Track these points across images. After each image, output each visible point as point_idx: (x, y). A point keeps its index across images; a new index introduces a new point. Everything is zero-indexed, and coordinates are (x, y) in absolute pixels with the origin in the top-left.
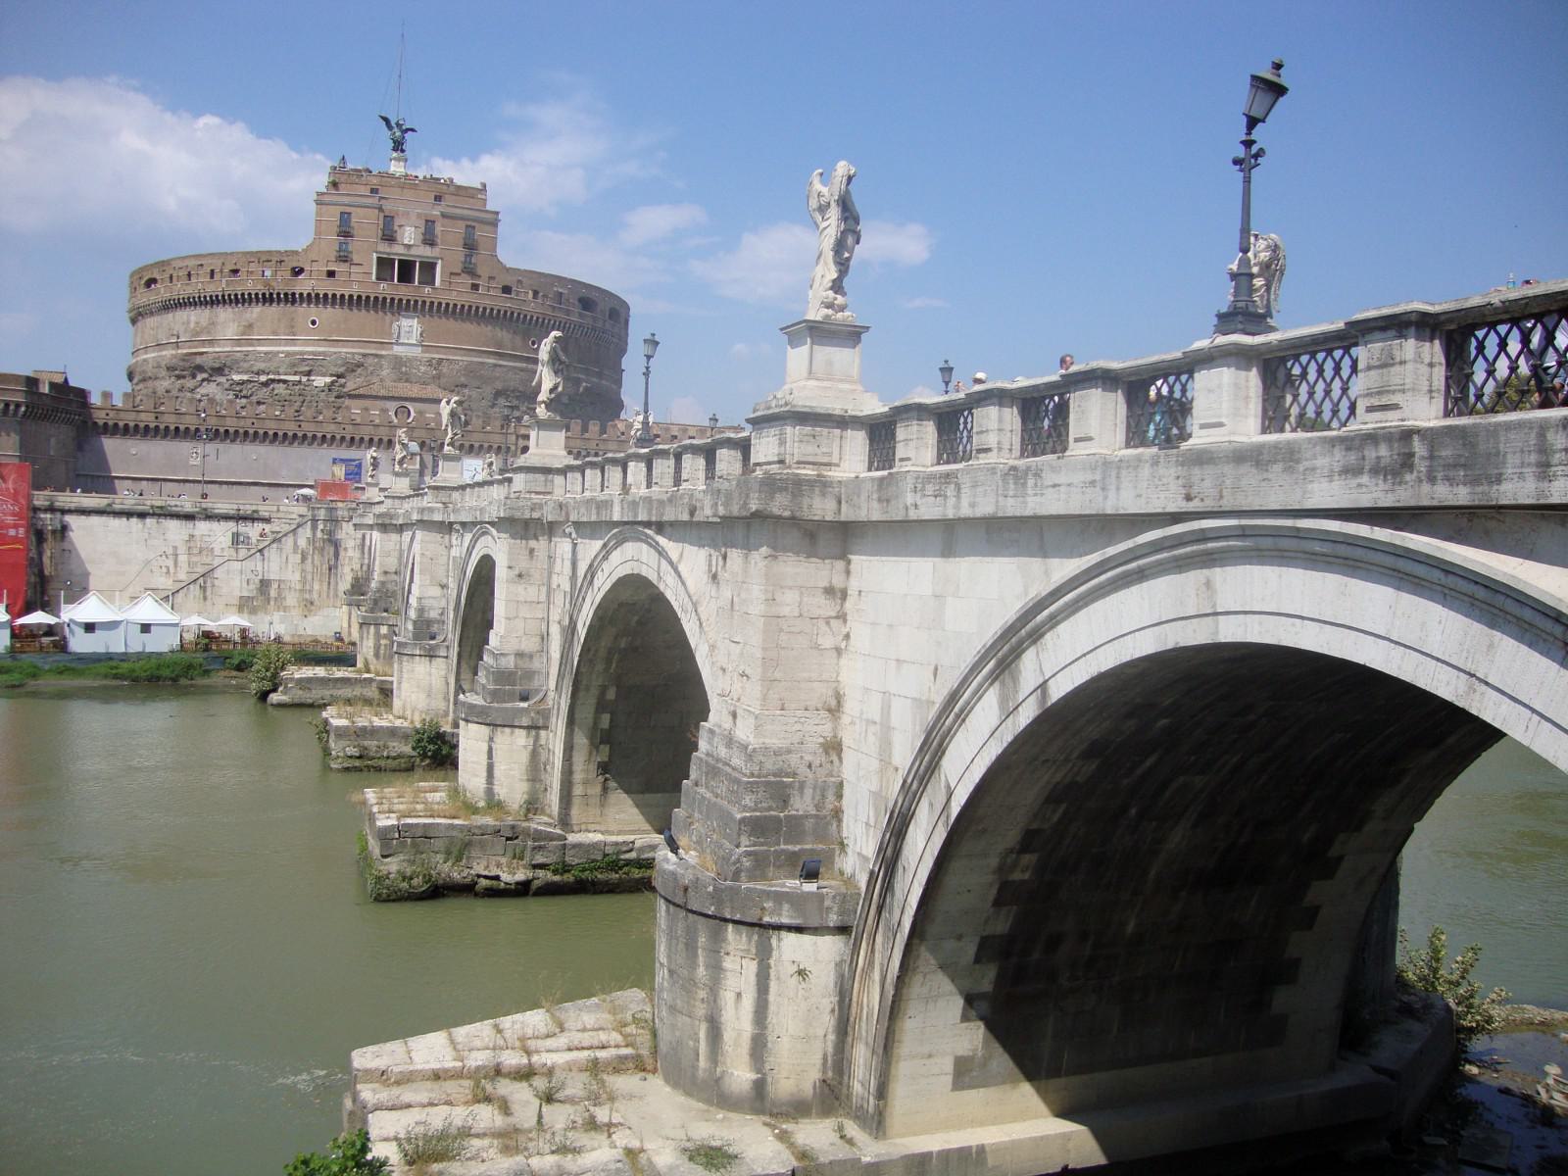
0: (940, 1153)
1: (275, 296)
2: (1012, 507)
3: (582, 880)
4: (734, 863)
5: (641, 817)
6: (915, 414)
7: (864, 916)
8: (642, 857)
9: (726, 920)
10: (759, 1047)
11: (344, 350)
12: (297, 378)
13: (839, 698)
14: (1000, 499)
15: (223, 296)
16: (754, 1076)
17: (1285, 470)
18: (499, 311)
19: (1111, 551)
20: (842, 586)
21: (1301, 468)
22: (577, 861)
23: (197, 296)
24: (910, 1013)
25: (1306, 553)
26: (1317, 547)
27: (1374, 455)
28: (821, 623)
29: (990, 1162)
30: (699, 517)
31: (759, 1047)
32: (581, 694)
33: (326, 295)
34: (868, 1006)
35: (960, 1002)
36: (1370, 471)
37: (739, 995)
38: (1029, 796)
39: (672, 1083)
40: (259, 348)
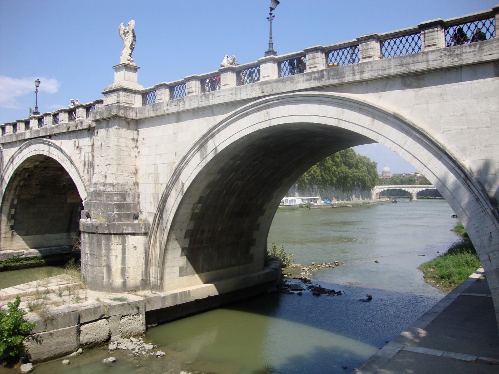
0: (180, 293)
2: (204, 104)
3: (6, 266)
4: (113, 217)
5: (25, 244)
6: (164, 87)
7: (153, 228)
8: (27, 257)
9: (111, 234)
10: (123, 271)
13: (136, 170)
14: (200, 102)
16: (123, 280)
17: (290, 82)
19: (244, 106)
20: (136, 138)
21: (295, 81)
22: (4, 260)
24: (169, 253)
25: (295, 101)
26: (299, 99)
27: (314, 76)
28: (131, 148)
29: (192, 295)
30: (70, 130)
31: (123, 271)
32: (5, 202)
34: (155, 254)
35: (180, 250)
36: (313, 79)
37: (116, 256)
38: (203, 186)
39: (94, 289)
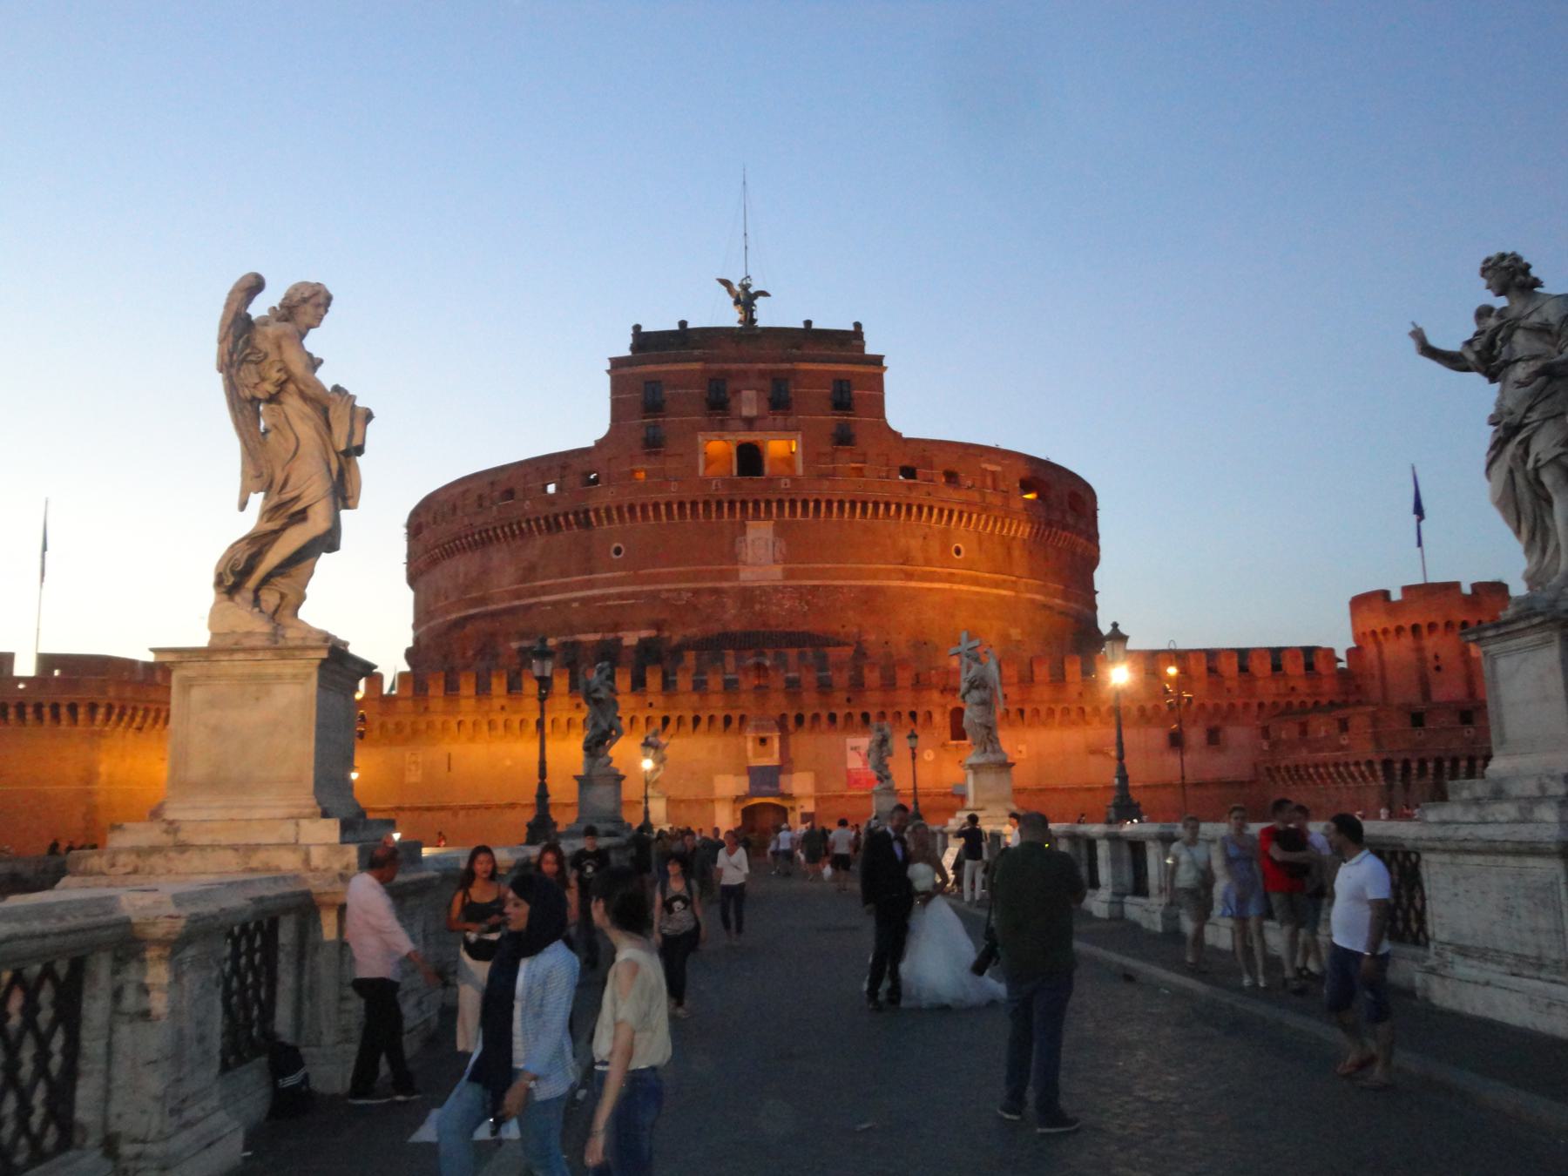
1: (561, 519)
11: (666, 586)
12: (598, 637)
15: (495, 529)
18: (899, 506)
23: (463, 534)
33: (632, 509)
40: (545, 599)
